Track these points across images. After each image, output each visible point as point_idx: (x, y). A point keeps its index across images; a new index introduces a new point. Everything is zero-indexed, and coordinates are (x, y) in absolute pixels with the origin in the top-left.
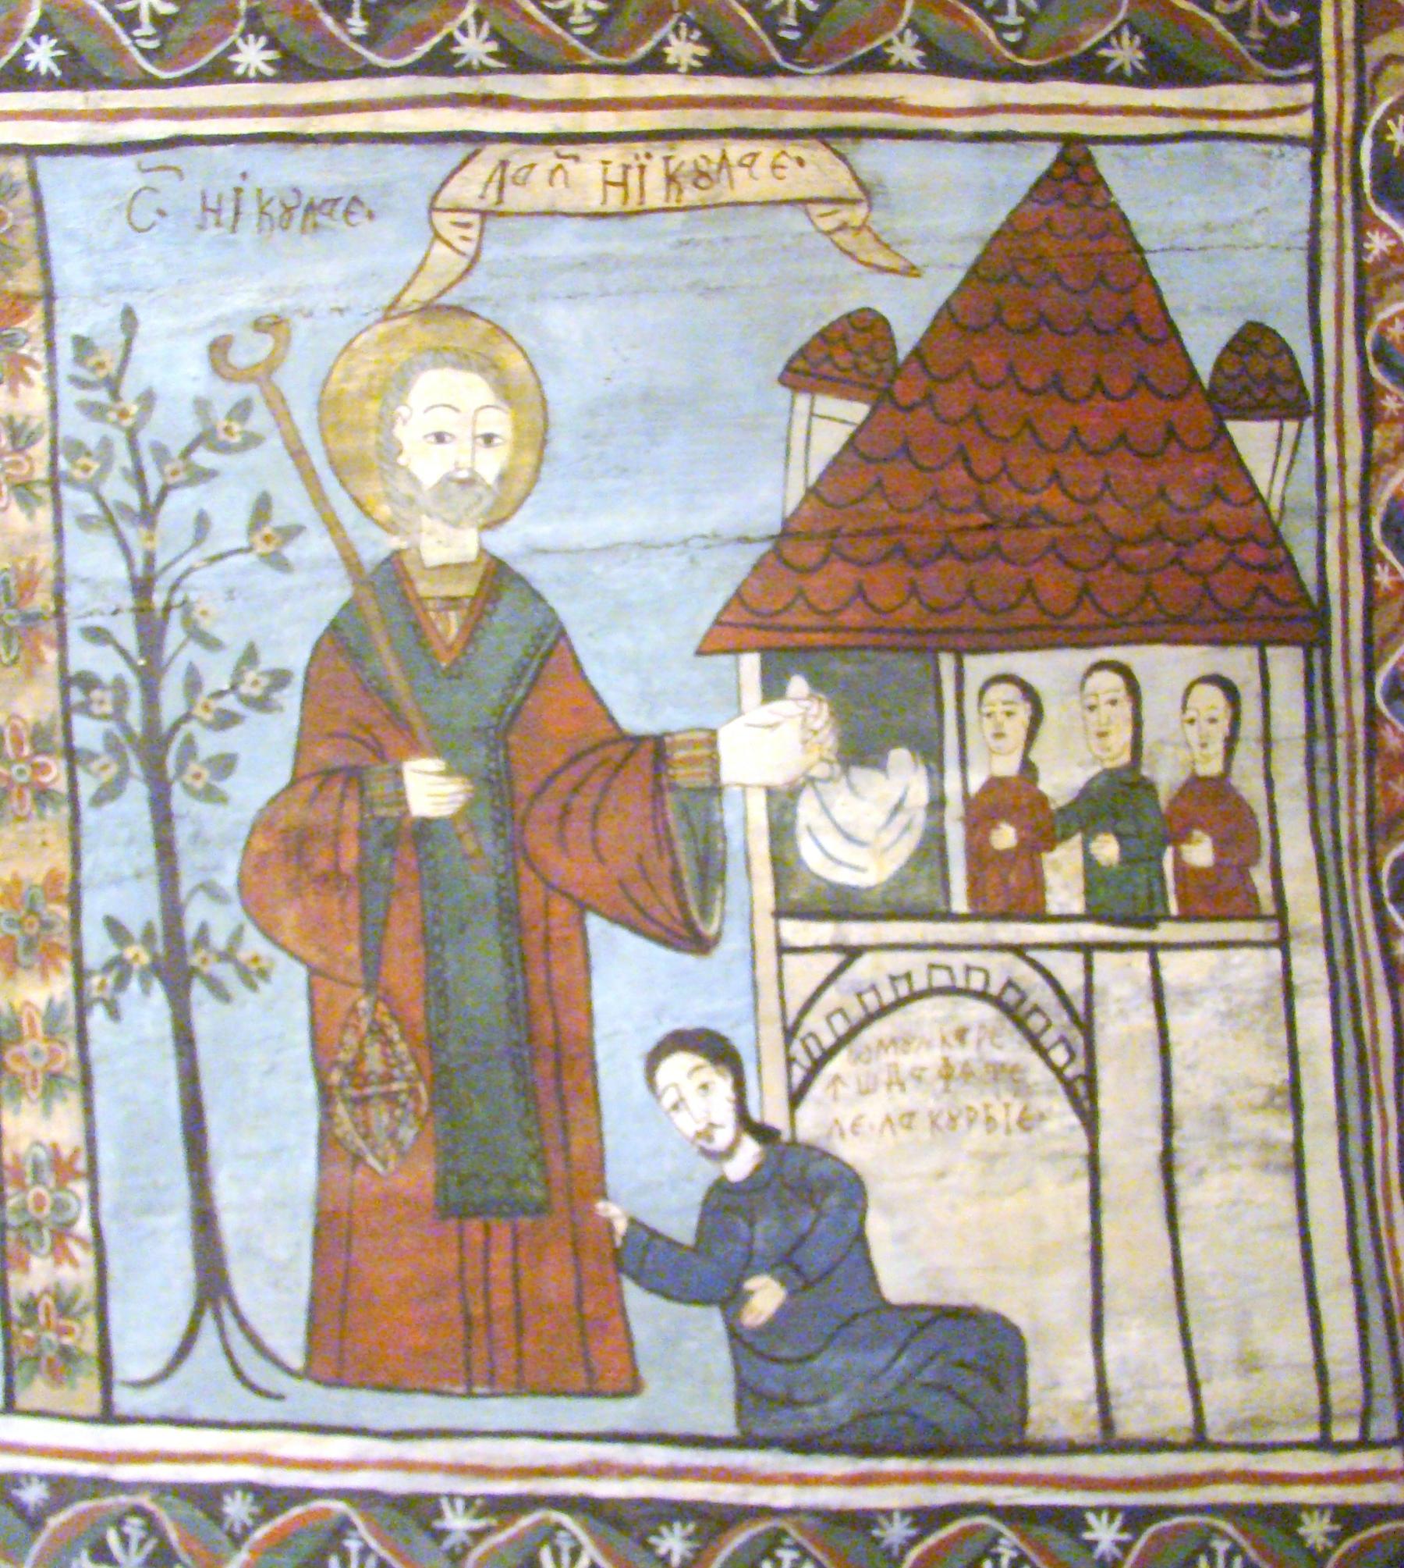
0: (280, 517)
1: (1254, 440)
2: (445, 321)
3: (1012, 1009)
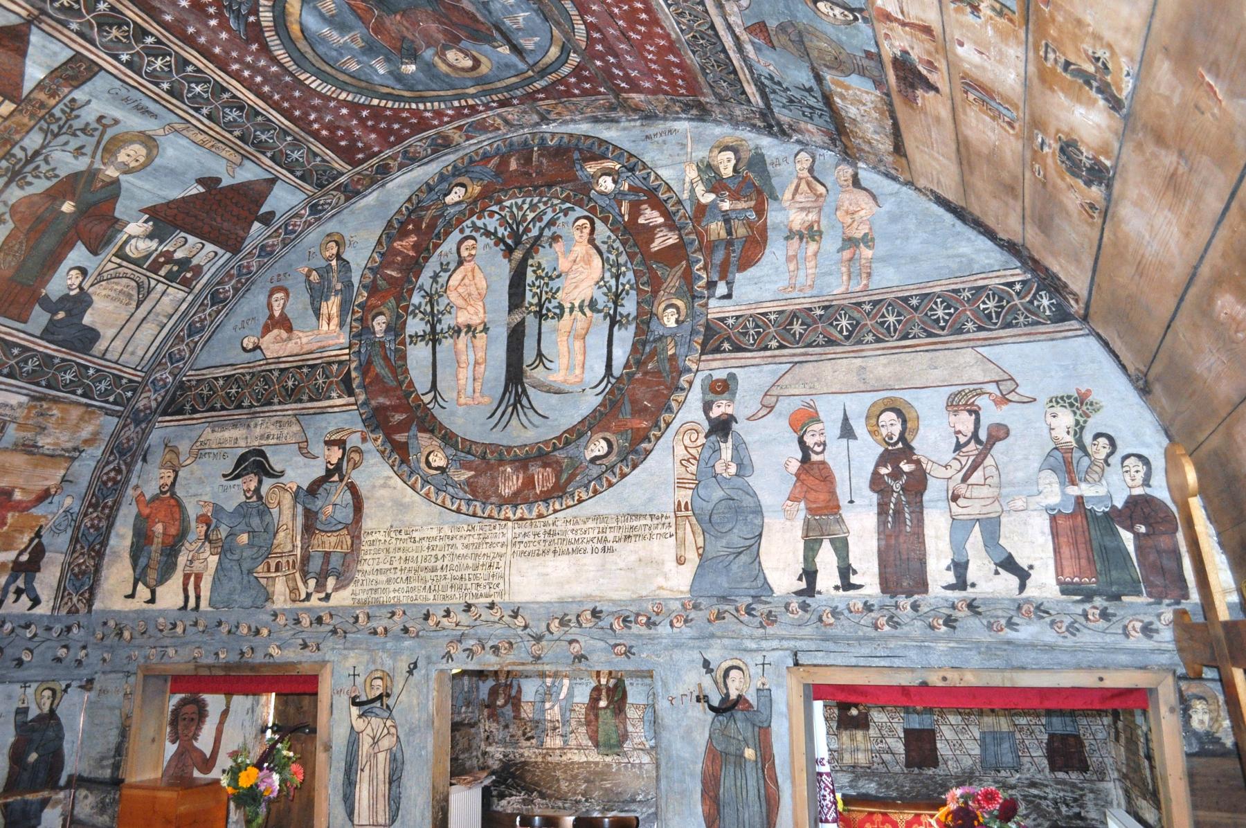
0: (84, 151)
1: (256, 225)
2: (149, 141)
3: (139, 286)
